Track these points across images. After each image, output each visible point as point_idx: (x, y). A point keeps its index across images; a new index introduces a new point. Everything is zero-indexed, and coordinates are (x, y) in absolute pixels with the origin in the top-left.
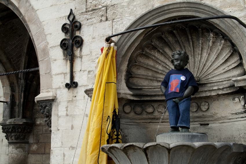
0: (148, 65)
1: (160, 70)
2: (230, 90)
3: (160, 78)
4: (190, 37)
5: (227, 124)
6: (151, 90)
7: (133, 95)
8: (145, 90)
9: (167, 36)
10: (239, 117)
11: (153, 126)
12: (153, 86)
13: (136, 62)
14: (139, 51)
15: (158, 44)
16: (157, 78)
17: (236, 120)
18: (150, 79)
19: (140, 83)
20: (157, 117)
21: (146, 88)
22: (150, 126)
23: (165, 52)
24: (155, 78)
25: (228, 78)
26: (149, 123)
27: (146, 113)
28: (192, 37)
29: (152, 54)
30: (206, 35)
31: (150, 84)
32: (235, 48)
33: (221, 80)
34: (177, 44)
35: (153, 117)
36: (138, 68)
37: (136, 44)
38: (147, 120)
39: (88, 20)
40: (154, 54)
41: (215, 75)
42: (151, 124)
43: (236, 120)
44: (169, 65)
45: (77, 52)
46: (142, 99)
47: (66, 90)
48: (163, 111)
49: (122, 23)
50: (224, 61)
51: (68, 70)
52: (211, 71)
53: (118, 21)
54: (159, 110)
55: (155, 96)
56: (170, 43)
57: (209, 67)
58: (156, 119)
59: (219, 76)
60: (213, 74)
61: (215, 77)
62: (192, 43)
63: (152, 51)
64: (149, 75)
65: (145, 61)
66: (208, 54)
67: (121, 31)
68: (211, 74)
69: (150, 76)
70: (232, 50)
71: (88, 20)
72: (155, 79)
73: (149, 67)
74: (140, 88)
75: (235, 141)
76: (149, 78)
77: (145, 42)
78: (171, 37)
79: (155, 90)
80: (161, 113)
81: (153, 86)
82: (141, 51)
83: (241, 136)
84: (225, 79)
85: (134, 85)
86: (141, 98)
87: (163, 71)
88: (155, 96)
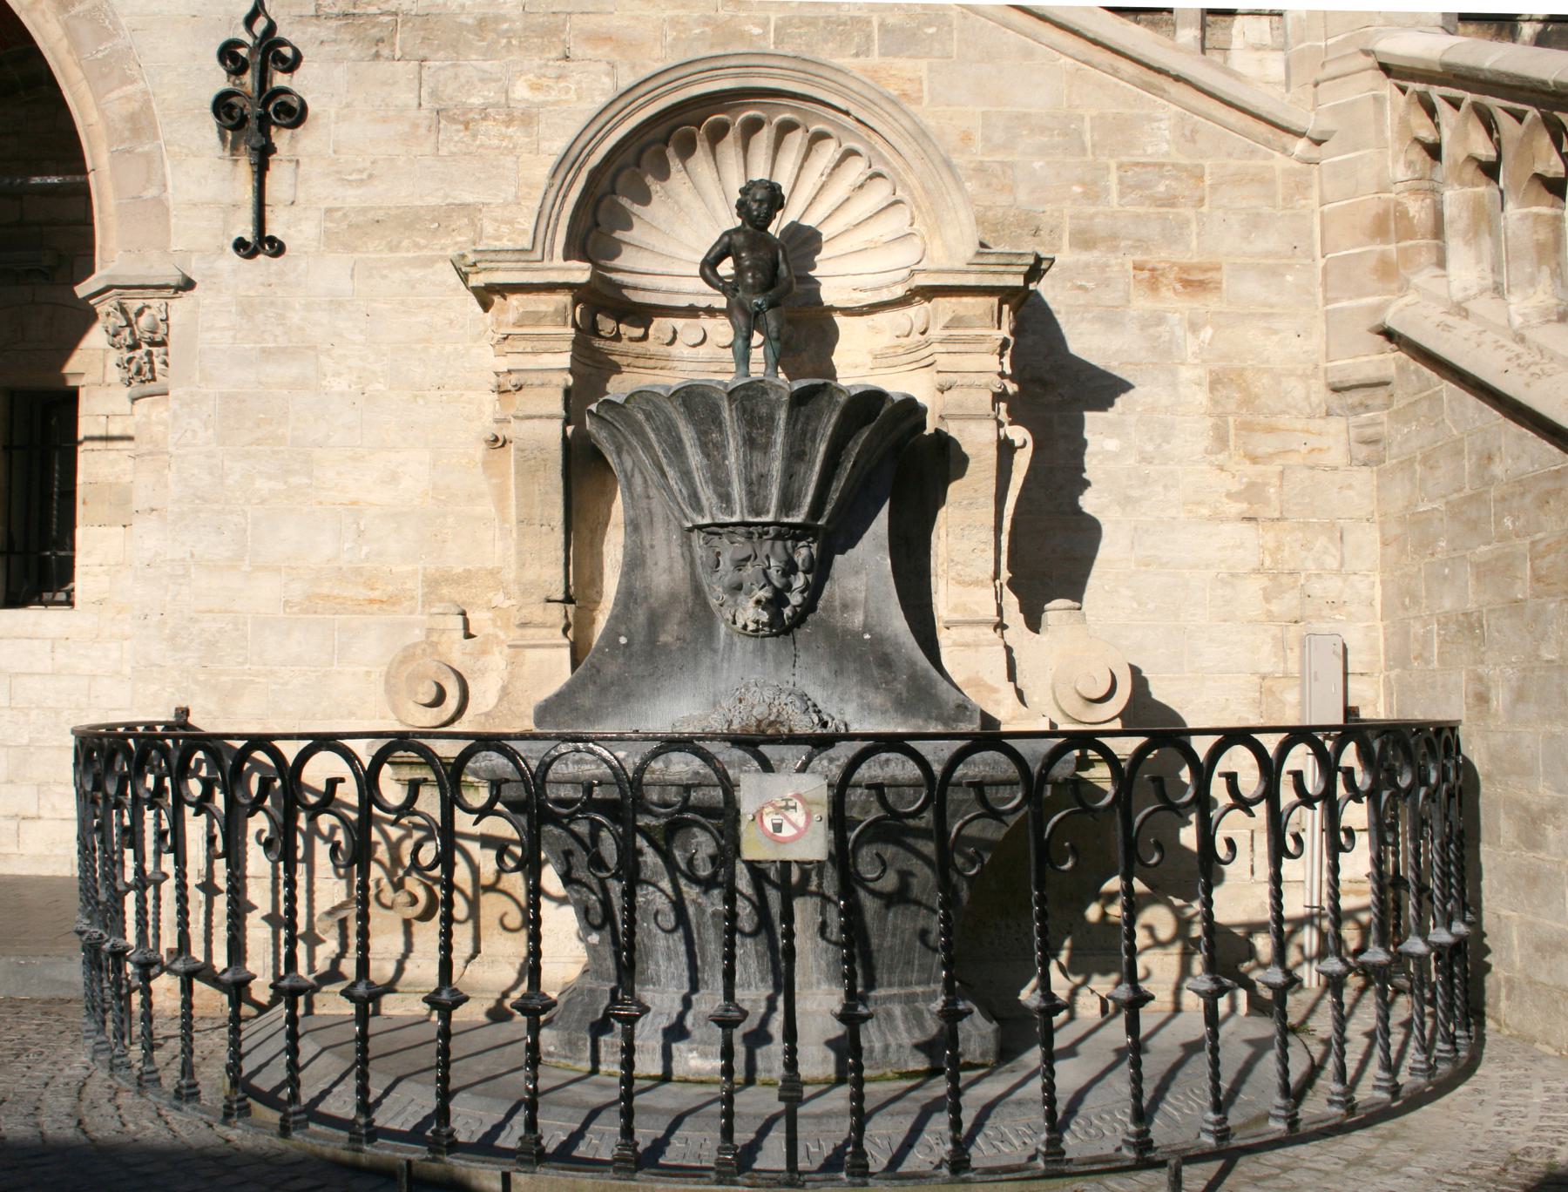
39: (322, 42)
45: (281, 138)
47: (236, 258)
49: (456, 77)
51: (247, 193)
53: (440, 68)
67: (451, 99)
71: (322, 42)
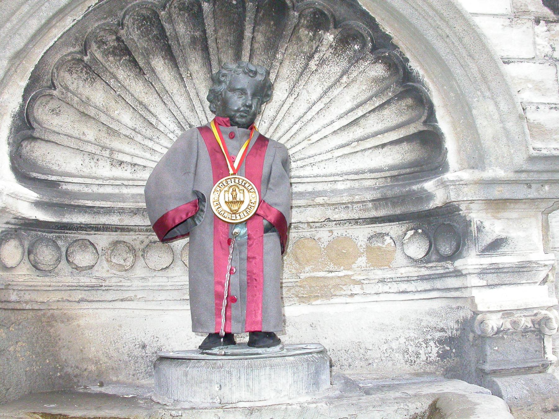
0: (86, 102)
4: (248, 34)
6: (90, 191)
7: (38, 204)
8: (70, 187)
9: (174, 16)
11: (91, 311)
12: (97, 178)
13: (53, 86)
14: (72, 50)
15: (136, 39)
16: (112, 150)
18: (90, 154)
19: (53, 162)
23: (153, 71)
25: (357, 173)
27: (70, 270)
28: (255, 34)
29: (109, 69)
30: (303, 38)
33: (332, 179)
34: (195, 49)
35: (94, 282)
36: (53, 111)
37: (68, 22)
40: (113, 70)
42: (84, 305)
50: (345, 121)
55: (109, 211)
56: (178, 41)
62: (248, 55)
63: (111, 58)
64: (86, 139)
65: (81, 90)
66: (294, 97)
70: (393, 92)
73: (92, 112)
74: (54, 178)
75: (367, 360)
76: (90, 148)
77: (97, 21)
78: (182, 25)
81: (97, 178)
82: (77, 48)
83: (394, 345)
85: (34, 166)
87: (134, 130)
88: (109, 211)
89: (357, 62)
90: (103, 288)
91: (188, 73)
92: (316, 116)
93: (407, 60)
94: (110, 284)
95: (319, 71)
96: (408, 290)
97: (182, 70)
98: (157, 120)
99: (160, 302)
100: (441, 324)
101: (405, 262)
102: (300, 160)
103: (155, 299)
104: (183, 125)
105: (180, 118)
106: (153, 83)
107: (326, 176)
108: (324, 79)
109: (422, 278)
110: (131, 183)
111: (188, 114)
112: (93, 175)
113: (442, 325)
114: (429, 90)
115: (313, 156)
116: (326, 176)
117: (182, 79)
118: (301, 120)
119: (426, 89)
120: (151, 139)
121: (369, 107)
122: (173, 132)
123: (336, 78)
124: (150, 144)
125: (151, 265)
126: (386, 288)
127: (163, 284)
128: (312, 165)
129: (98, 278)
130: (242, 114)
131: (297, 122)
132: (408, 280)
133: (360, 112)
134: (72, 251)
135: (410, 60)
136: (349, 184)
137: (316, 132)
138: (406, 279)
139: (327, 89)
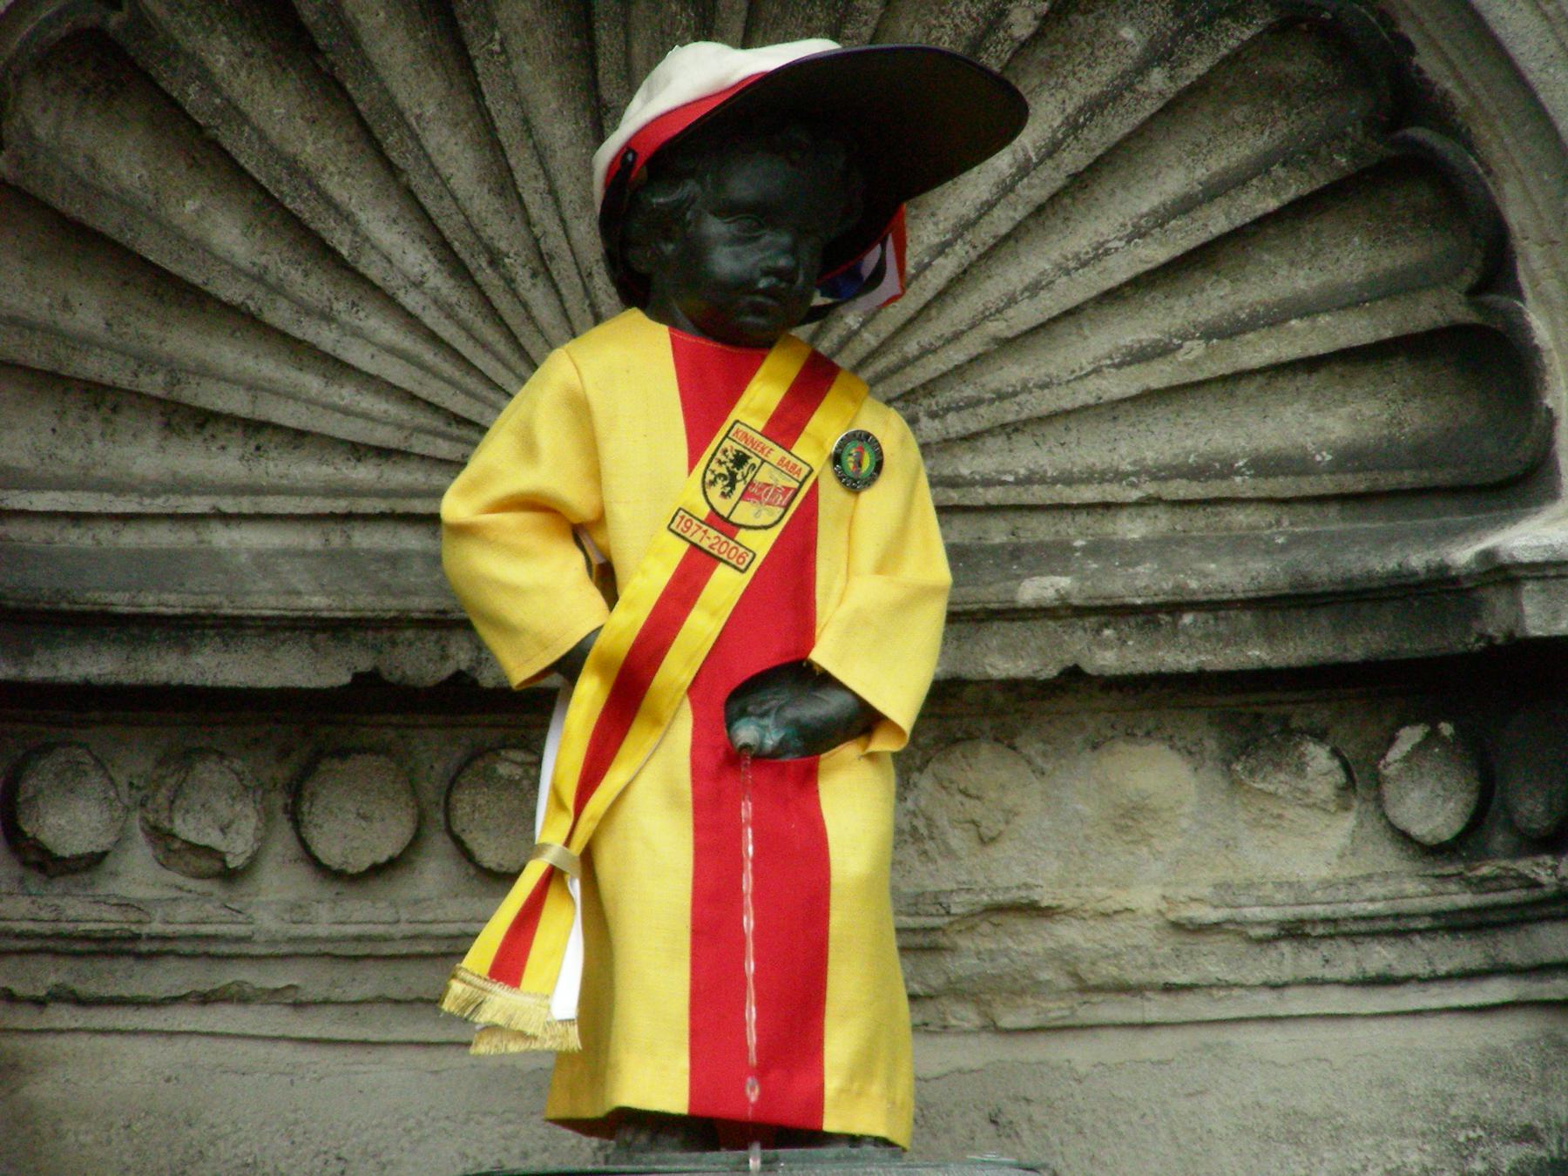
1: (237, 271)
2: (1270, 637)
3: (204, 371)
5: (1111, 1047)
10: (1329, 973)
11: (83, 1042)
12: (117, 487)
16: (175, 370)
17: (1267, 1003)
20: (156, 927)
21: (42, 501)
22: (49, 1040)
24: (159, 378)
25: (1196, 473)
26: (40, 1003)
31: (72, 456)
32: (1419, 133)
33: (1089, 494)
35: (110, 920)
38: (32, 963)
40: (195, 42)
41: (1009, 412)
42: (63, 1016)
43: (1267, 1003)
44: (353, 206)
46: (34, 673)
48: (237, 849)
50: (1156, 253)
52: (957, 355)
54: (188, 828)
57: (928, 295)
58: (139, 956)
59: (1053, 432)
60: (969, 391)
61: (991, 443)
68: (944, 398)
69: (84, 343)
70: (1354, 154)
72: (153, 384)
76: (94, 367)
79: (130, 538)
80: (205, 864)
81: (117, 487)
84: (1150, 488)
86: (24, 654)
89: (1209, 20)
90: (144, 947)
91: (491, 40)
92: (1031, 222)
93: (1409, 48)
94: (169, 930)
95: (1050, 37)
96: (1401, 971)
97: (469, 26)
98: (355, 233)
99: (352, 1009)
100: (1525, 1110)
101: (1389, 858)
102: (958, 409)
103: (336, 994)
104: (464, 255)
105: (451, 227)
106: (349, 86)
107: (1069, 480)
108: (1069, 67)
109: (1453, 924)
110: (246, 505)
111: (482, 202)
112: (101, 472)
113: (1524, 1115)
114: (1489, 172)
115: (1015, 394)
116: (1069, 480)
117: (467, 64)
118: (969, 236)
119: (1481, 163)
120: (327, 317)
121: (1259, 202)
122: (418, 285)
123: (1120, 68)
124: (326, 338)
125: (330, 850)
126: (1310, 962)
127: (380, 930)
128: (1009, 430)
129: (125, 905)
130: (759, 299)
131: (948, 244)
132: (1397, 928)
133: (1217, 221)
134: (31, 791)
135: (1418, 46)
136: (1162, 522)
137: (1034, 289)
138: (1389, 924)
139: (1080, 110)
